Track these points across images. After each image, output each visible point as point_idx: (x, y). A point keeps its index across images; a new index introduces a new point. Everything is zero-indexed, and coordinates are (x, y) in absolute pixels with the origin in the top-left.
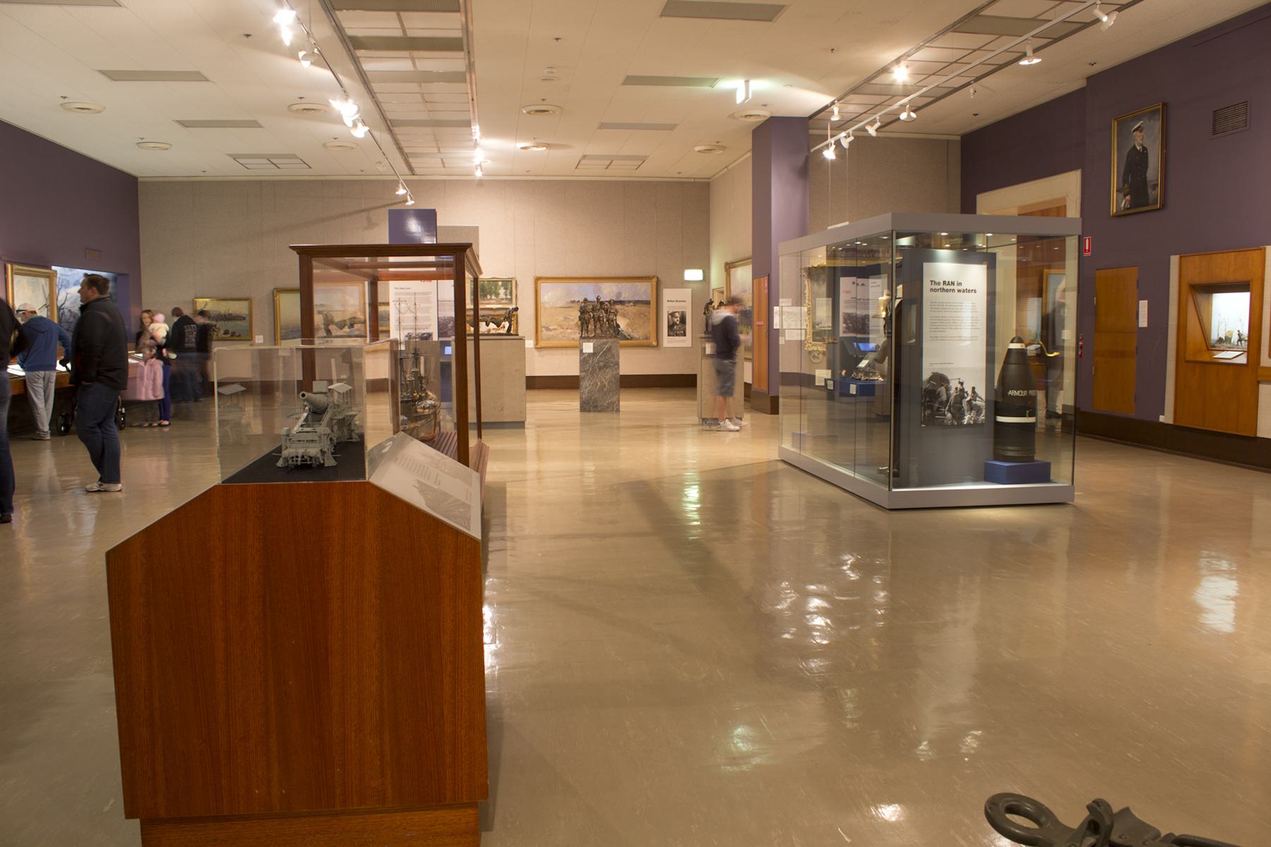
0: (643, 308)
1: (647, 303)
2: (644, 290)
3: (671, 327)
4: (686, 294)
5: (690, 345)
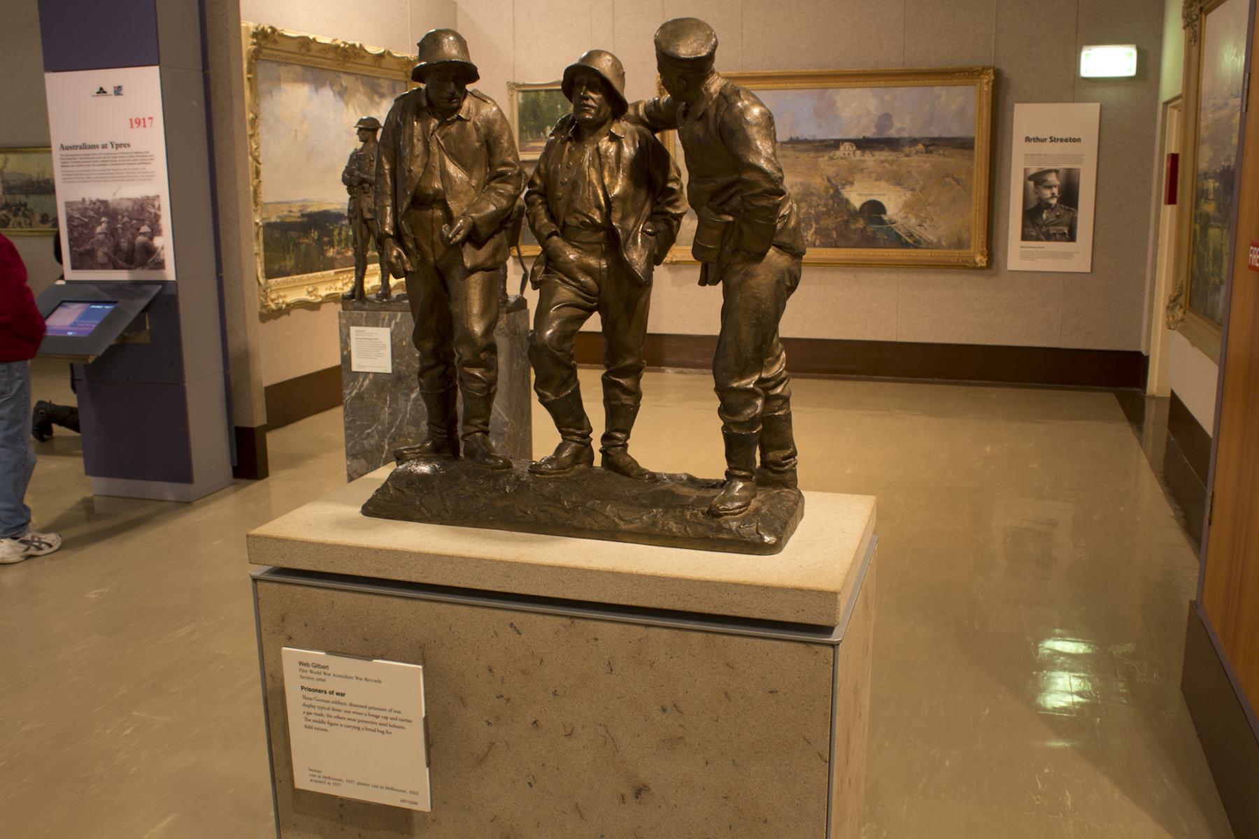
0: (953, 160)
1: (965, 145)
2: (957, 109)
3: (1032, 214)
4: (1083, 118)
5: (1086, 267)
